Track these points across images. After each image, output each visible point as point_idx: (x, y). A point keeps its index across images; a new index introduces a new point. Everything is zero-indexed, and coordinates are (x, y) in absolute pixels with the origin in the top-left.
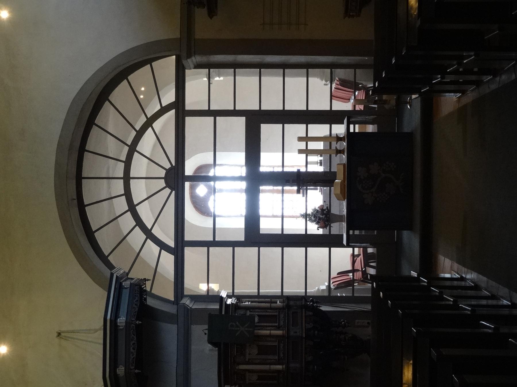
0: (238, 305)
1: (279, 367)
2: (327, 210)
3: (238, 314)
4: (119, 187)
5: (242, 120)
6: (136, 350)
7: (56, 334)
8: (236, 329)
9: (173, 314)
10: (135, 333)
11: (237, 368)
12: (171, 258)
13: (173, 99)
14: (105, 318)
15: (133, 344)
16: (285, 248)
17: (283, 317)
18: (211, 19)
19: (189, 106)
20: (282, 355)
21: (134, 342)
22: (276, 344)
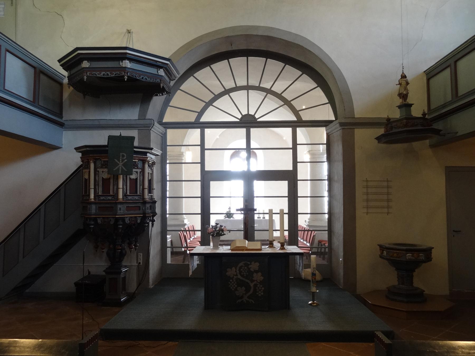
0: (146, 162)
1: (92, 196)
2: (223, 233)
3: (138, 162)
4: (242, 82)
5: (290, 168)
6: (102, 76)
7: (129, 29)
8: (121, 159)
9: (145, 116)
10: (117, 75)
11: (91, 162)
12: (193, 120)
13: (304, 119)
14: (127, 48)
15: (108, 74)
16: (200, 199)
17: (135, 199)
18: (375, 139)
19: (299, 130)
20: (102, 198)
21: (109, 74)
22: (111, 193)
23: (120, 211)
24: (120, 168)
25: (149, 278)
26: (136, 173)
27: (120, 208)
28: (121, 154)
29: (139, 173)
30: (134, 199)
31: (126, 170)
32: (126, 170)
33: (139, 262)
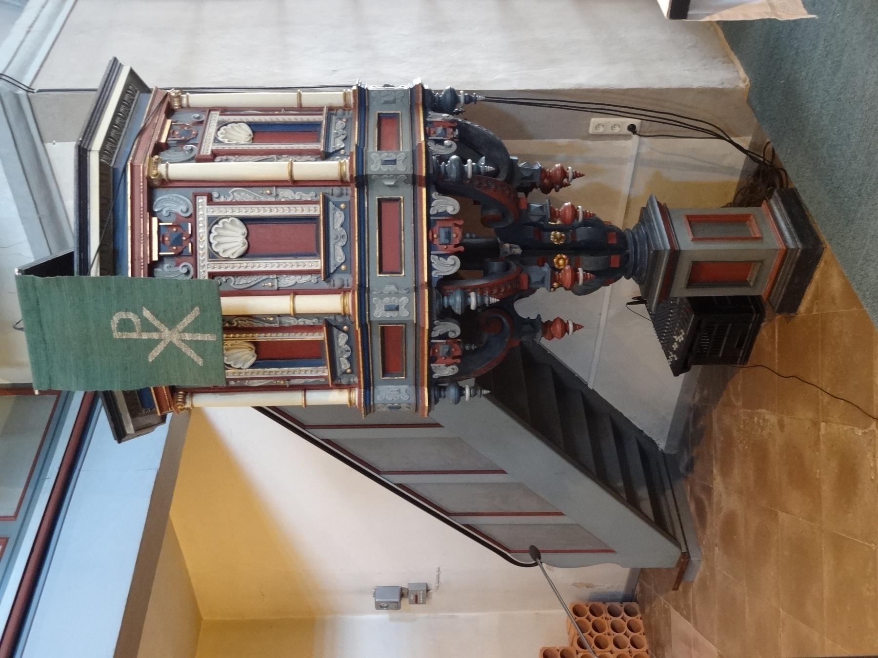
1: (338, 397)
3: (164, 213)
8: (145, 336)
23: (402, 308)
24: (188, 337)
25: (703, 92)
26: (217, 223)
27: (386, 310)
28: (117, 335)
29: (217, 211)
30: (344, 232)
31: (196, 312)
32: (196, 312)
33: (626, 131)
